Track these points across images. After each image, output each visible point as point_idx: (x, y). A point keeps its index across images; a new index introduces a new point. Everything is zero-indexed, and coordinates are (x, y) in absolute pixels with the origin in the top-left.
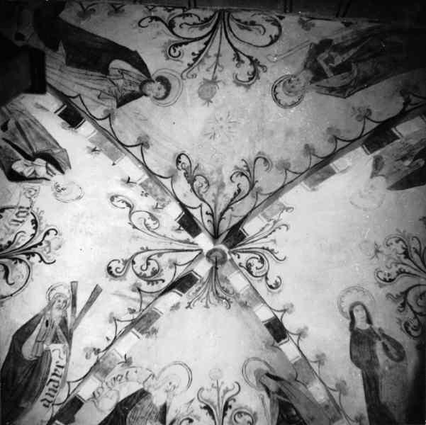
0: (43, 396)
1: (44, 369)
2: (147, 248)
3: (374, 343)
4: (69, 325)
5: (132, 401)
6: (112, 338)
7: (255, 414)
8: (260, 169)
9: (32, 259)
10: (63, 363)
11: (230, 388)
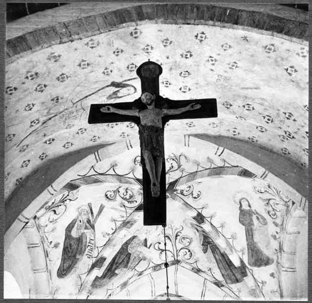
0: (85, 254)
1: (84, 241)
3: (252, 216)
4: (91, 222)
7: (191, 238)
8: (182, 158)
9: (66, 202)
10: (93, 238)
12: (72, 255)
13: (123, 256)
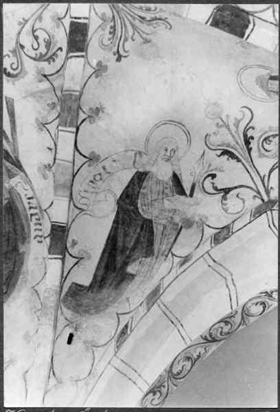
0: (33, 234)
1: (20, 208)
2: (23, 19)
4: (11, 154)
5: (133, 189)
6: (53, 146)
11: (239, 117)
12: (10, 248)
13: (131, 231)
